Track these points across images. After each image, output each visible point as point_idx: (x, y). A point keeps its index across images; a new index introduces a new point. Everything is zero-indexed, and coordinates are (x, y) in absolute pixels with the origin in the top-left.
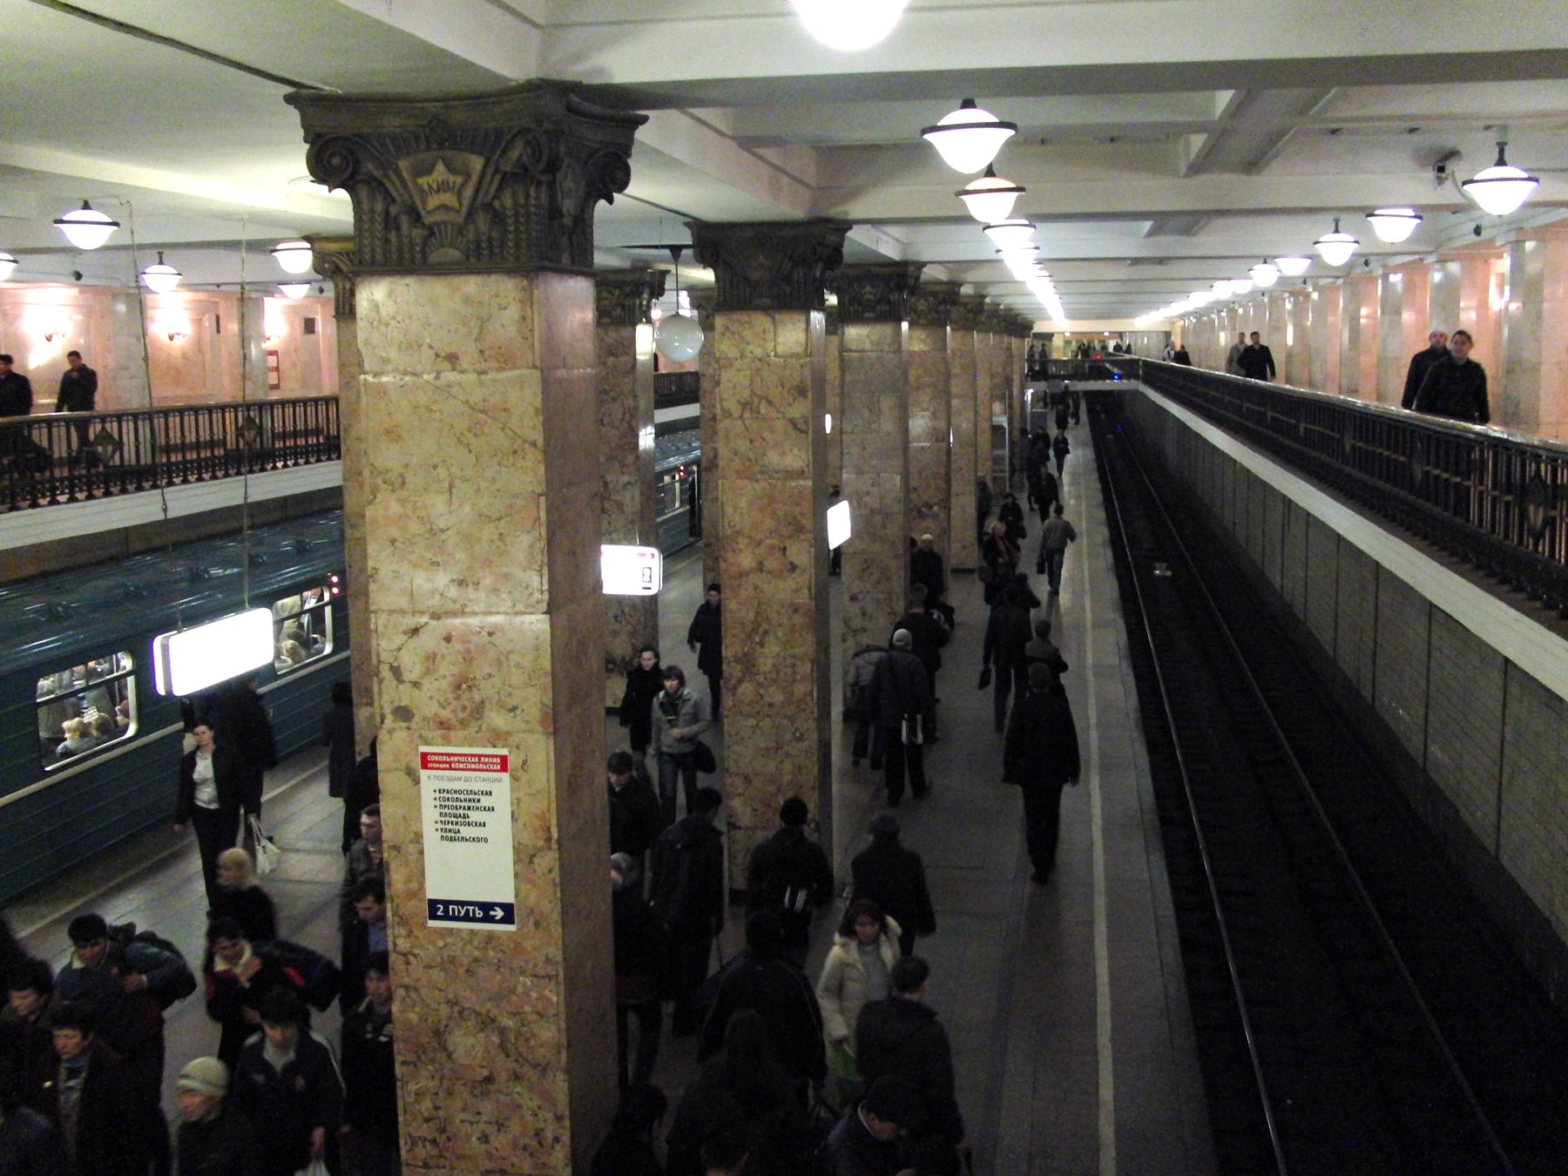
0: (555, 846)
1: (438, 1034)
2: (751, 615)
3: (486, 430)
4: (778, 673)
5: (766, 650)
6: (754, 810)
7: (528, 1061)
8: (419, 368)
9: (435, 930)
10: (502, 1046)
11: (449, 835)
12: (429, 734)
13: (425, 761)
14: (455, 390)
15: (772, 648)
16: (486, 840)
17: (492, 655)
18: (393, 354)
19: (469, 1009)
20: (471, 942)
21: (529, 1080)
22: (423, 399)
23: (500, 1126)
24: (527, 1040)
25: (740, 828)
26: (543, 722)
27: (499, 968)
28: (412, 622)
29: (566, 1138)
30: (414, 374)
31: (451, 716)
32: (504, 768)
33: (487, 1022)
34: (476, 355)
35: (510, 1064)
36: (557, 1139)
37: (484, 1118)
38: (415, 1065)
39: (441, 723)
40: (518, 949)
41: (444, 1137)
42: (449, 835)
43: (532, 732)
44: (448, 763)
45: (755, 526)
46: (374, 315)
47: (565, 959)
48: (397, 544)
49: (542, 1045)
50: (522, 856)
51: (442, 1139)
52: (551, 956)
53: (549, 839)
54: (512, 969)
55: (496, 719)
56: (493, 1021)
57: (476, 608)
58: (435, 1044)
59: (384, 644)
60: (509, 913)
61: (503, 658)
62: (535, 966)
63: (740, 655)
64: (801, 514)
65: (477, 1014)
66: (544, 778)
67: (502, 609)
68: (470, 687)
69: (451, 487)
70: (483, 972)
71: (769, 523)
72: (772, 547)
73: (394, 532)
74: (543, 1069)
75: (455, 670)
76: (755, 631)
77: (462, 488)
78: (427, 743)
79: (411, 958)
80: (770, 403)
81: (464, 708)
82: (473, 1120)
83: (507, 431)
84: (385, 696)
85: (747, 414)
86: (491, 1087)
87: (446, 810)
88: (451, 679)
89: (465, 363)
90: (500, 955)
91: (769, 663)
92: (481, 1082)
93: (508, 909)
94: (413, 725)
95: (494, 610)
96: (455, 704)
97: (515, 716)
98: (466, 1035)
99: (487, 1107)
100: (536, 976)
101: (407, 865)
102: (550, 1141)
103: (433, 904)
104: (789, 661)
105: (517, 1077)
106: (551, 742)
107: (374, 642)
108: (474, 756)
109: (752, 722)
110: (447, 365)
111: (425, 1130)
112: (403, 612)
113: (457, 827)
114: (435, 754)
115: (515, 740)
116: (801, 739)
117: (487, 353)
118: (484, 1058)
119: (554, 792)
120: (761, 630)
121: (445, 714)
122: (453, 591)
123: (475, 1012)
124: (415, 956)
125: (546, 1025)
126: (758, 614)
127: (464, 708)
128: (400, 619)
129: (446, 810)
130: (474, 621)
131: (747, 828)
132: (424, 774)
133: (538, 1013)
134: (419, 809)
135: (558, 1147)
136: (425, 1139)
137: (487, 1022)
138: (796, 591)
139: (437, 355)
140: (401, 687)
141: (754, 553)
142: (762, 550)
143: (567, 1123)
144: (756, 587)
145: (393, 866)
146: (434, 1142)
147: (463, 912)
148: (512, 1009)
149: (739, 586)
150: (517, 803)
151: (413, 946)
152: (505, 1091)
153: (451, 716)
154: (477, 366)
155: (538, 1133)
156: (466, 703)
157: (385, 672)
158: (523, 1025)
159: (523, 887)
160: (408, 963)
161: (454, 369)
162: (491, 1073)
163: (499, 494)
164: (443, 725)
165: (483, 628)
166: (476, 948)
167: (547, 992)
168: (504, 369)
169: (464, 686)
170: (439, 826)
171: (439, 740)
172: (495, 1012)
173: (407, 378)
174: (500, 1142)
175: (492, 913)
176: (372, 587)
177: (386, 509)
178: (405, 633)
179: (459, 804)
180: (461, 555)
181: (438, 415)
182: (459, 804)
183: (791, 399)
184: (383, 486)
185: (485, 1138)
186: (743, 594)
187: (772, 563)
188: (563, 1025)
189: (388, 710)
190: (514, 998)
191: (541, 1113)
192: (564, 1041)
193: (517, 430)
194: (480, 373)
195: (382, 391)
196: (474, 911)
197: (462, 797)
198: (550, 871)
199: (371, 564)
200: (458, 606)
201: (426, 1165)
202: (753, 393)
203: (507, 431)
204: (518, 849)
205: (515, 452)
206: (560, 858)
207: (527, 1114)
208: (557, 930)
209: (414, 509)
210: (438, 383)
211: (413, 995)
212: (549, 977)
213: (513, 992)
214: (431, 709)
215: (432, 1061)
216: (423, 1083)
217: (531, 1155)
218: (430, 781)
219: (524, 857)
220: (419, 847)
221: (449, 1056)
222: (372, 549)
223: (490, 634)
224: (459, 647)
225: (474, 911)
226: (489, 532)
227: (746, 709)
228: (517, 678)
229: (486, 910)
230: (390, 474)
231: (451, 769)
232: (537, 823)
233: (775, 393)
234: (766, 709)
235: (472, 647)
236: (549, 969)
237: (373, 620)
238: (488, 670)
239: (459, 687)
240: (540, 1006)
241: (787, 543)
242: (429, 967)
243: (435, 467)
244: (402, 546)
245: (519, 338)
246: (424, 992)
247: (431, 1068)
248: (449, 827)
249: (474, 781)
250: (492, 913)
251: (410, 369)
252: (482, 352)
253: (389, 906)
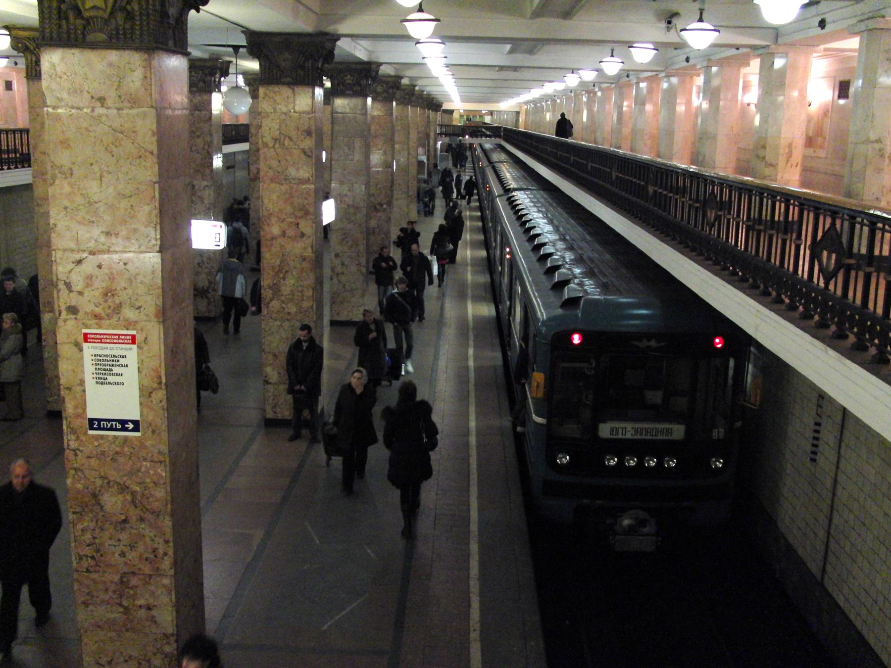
0: (164, 387)
1: (95, 496)
2: (278, 262)
3: (123, 143)
6: (279, 373)
7: (147, 509)
8: (81, 105)
9: (93, 436)
10: (133, 501)
11: (101, 381)
12: (89, 322)
13: (86, 338)
14: (104, 119)
15: (291, 281)
16: (123, 384)
17: (126, 276)
18: (65, 95)
19: (113, 481)
20: (114, 442)
21: (149, 521)
22: (85, 125)
23: (132, 547)
24: (147, 498)
25: (270, 383)
26: (157, 316)
27: (130, 458)
28: (78, 256)
29: (171, 552)
30: (78, 108)
31: (101, 311)
32: (134, 342)
33: (123, 488)
34: (117, 99)
35: (138, 512)
36: (165, 554)
37: (122, 543)
38: (81, 515)
39: (95, 316)
40: (143, 446)
41: (99, 554)
42: (101, 381)
43: (149, 321)
44: (101, 339)
45: (281, 211)
46: (53, 71)
47: (170, 451)
48: (68, 210)
49: (157, 500)
50: (145, 393)
51: (97, 556)
52: (161, 450)
53: (160, 383)
54: (139, 458)
55: (129, 313)
56: (127, 488)
57: (117, 249)
58: (93, 502)
59: (60, 269)
60: (137, 425)
61: (133, 279)
62: (152, 456)
63: (271, 285)
64: (307, 204)
65: (118, 484)
66: (158, 347)
67: (132, 249)
68: (113, 295)
69: (101, 176)
70: (121, 460)
71: (289, 209)
72: (291, 223)
73: (66, 203)
74: (157, 514)
75: (104, 285)
76: (280, 271)
77: (107, 178)
78: (87, 327)
79: (78, 452)
80: (290, 138)
81: (110, 307)
82: (116, 544)
83: (136, 144)
84: (61, 300)
85: (277, 146)
86: (127, 525)
87: (99, 367)
88: (102, 290)
89: (109, 102)
90: (131, 450)
91: (288, 289)
92: (120, 523)
93: (136, 423)
94: (79, 317)
95: (127, 250)
96: (106, 305)
97: (140, 312)
98: (111, 495)
99: (124, 536)
100: (152, 461)
101: (75, 398)
102: (161, 555)
103: (91, 421)
104: (300, 289)
105: (142, 520)
106: (161, 327)
107: (54, 268)
108: (116, 335)
109: (278, 323)
110: (98, 104)
111: (88, 551)
112: (72, 251)
113: (105, 376)
114: (92, 334)
115: (139, 326)
117: (123, 97)
118: (122, 509)
119: (163, 356)
120: (284, 271)
121: (98, 310)
122: (103, 239)
123: (117, 483)
124: (81, 451)
125: (159, 489)
126: (282, 261)
127: (110, 307)
128: (71, 254)
129: (99, 367)
130: (116, 257)
131: (275, 384)
132: (85, 346)
133: (154, 483)
134: (83, 366)
135: (166, 558)
136: (87, 556)
137: (123, 488)
138: (305, 248)
139: (92, 97)
140: (71, 294)
141: (280, 226)
142: (284, 225)
143: (171, 544)
144: (281, 246)
145: (67, 400)
146: (93, 557)
147: (109, 425)
148: (139, 480)
149: (272, 245)
150: (141, 362)
151: (80, 445)
152: (135, 527)
153: (101, 311)
154: (117, 105)
155: (154, 550)
156: (111, 304)
157: (61, 286)
158: (145, 490)
159: (145, 410)
160: (76, 455)
161: (102, 106)
162: (127, 517)
163: (130, 182)
164: (97, 316)
165: (120, 260)
166: (117, 446)
167: (159, 470)
168: (133, 108)
169: (109, 294)
170: (95, 376)
171: (95, 326)
172: (128, 483)
173: (74, 111)
174: (132, 556)
175: (126, 426)
176: (53, 235)
177: (61, 188)
178: (73, 263)
179: (106, 363)
180: (107, 217)
181: (92, 134)
182: (106, 363)
183: (303, 137)
184: (59, 175)
185: (123, 554)
186: (274, 250)
188: (169, 489)
189: (63, 307)
190: (140, 474)
191: (157, 539)
192: (169, 498)
193: (141, 144)
194: (118, 109)
195: (58, 118)
196: (116, 425)
197: (108, 359)
198: (161, 402)
199: (52, 221)
200: (105, 247)
201: (88, 571)
202: (281, 133)
203: (136, 144)
204: (141, 389)
205: (140, 157)
206: (167, 394)
207: (148, 540)
208: (165, 435)
209: (79, 189)
210: (93, 114)
211: (80, 474)
212: (161, 462)
213: (139, 470)
214: (90, 308)
215: (92, 511)
216: (86, 524)
217: (151, 563)
218: (89, 349)
219: (146, 393)
220: (82, 388)
221: (102, 508)
222: (53, 213)
223: (125, 264)
224: (107, 271)
225: (116, 425)
226: (124, 204)
227: (274, 316)
228: (141, 290)
229: (123, 424)
230: (63, 168)
231: (101, 342)
232: (153, 374)
233: (293, 134)
234: (286, 316)
235: (114, 272)
236: (160, 457)
237: (54, 255)
238: (123, 285)
239: (106, 295)
240: (155, 478)
241: (299, 221)
242: (89, 457)
243: (92, 164)
244: (71, 211)
245: (143, 89)
246: (87, 472)
247: (90, 515)
248: (101, 376)
249: (115, 350)
250: (126, 426)
251: (75, 105)
252: (120, 97)
253: (64, 422)
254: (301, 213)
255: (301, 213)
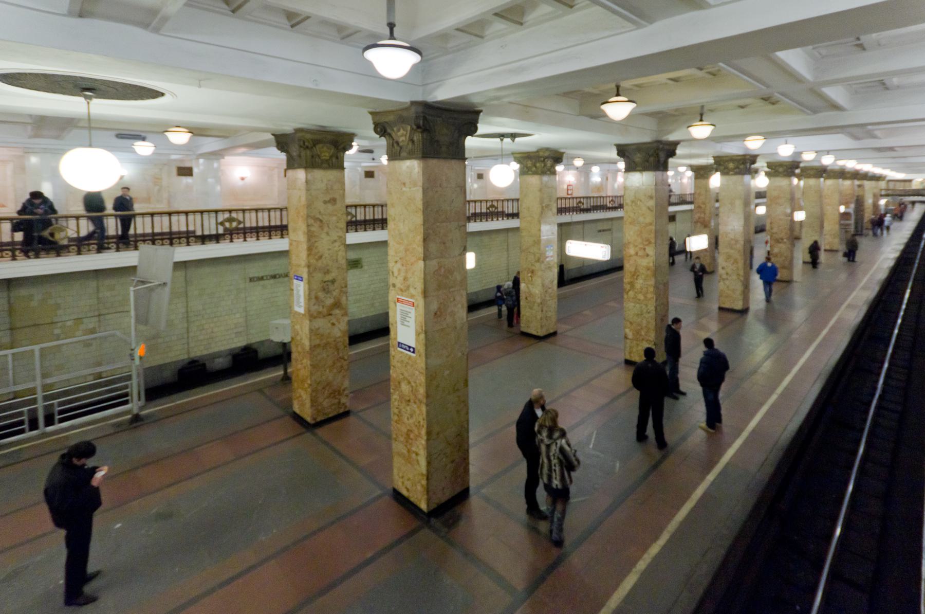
2: (633, 270)
4: (642, 289)
5: (638, 281)
76: (633, 275)
80: (641, 201)
85: (634, 204)
104: (646, 286)
116: (649, 313)
120: (636, 275)
126: (636, 269)
138: (648, 263)
142: (637, 249)
186: (631, 262)
187: (640, 253)
234: (638, 301)
241: (647, 247)
254: (647, 243)
255: (647, 243)
